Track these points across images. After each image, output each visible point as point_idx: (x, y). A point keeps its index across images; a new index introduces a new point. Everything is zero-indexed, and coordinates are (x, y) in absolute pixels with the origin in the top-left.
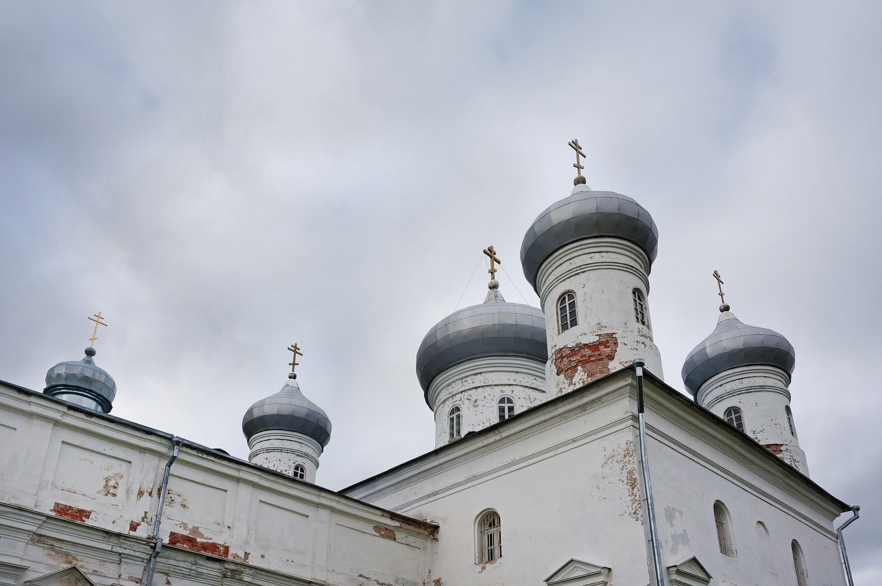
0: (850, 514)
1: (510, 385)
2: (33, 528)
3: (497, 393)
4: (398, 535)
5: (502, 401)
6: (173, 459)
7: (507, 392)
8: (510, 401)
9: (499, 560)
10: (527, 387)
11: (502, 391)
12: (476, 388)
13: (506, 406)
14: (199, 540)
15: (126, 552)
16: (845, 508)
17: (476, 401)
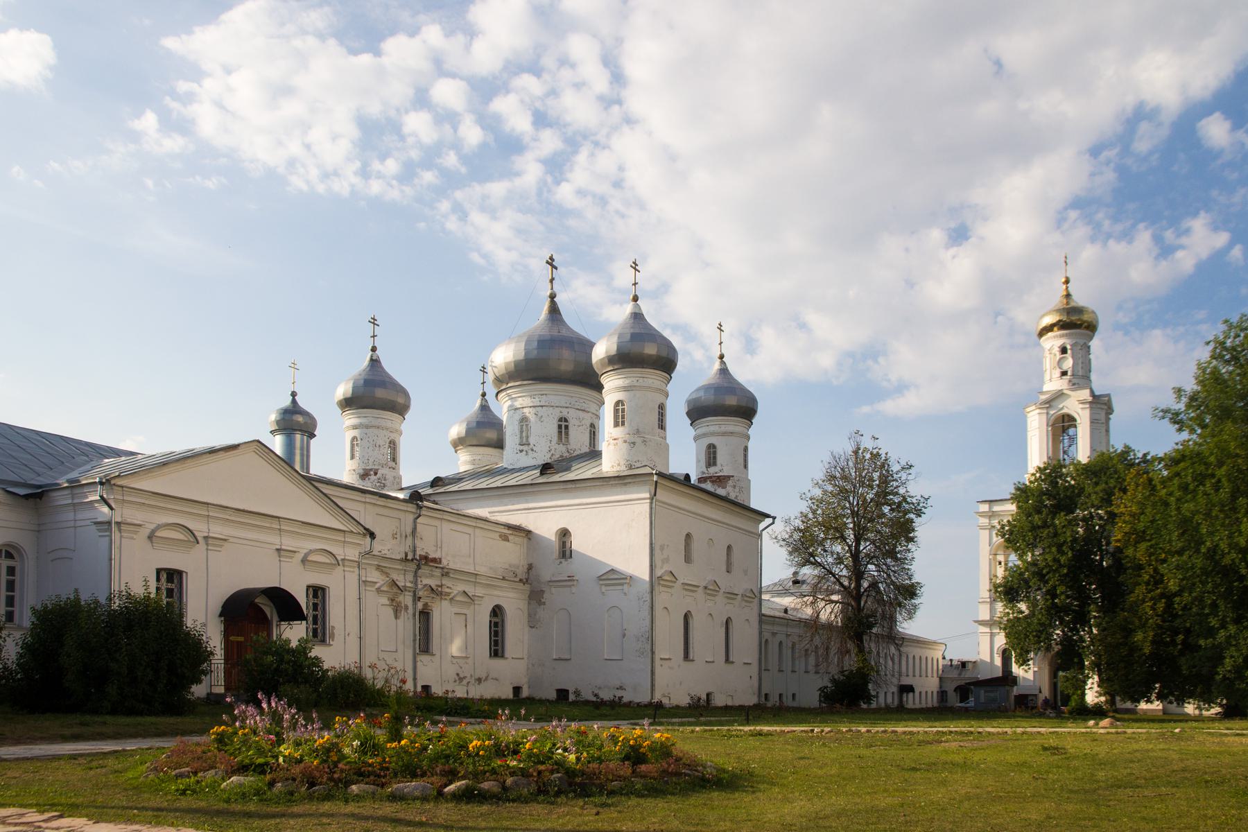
0: (769, 521)
1: (566, 407)
2: (376, 563)
3: (557, 413)
4: (511, 538)
5: (560, 420)
6: (420, 516)
7: (565, 413)
8: (566, 420)
9: (570, 560)
10: (578, 409)
11: (561, 412)
12: (542, 406)
13: (563, 424)
14: (430, 557)
15: (408, 569)
16: (768, 516)
17: (542, 417)
